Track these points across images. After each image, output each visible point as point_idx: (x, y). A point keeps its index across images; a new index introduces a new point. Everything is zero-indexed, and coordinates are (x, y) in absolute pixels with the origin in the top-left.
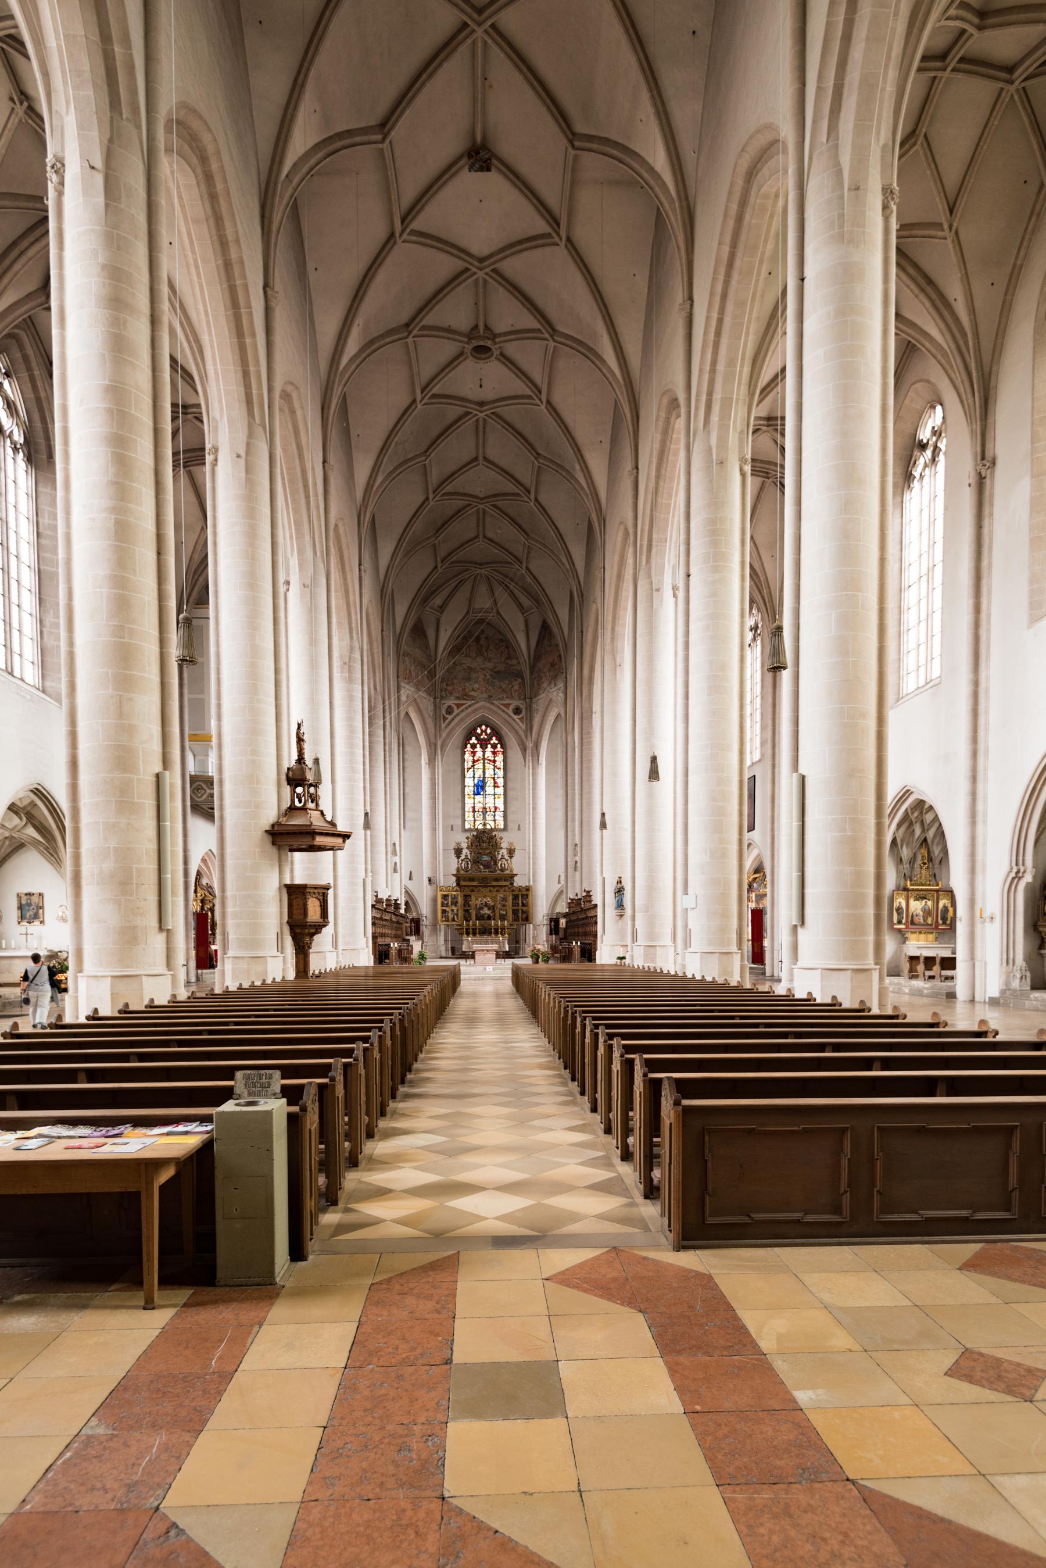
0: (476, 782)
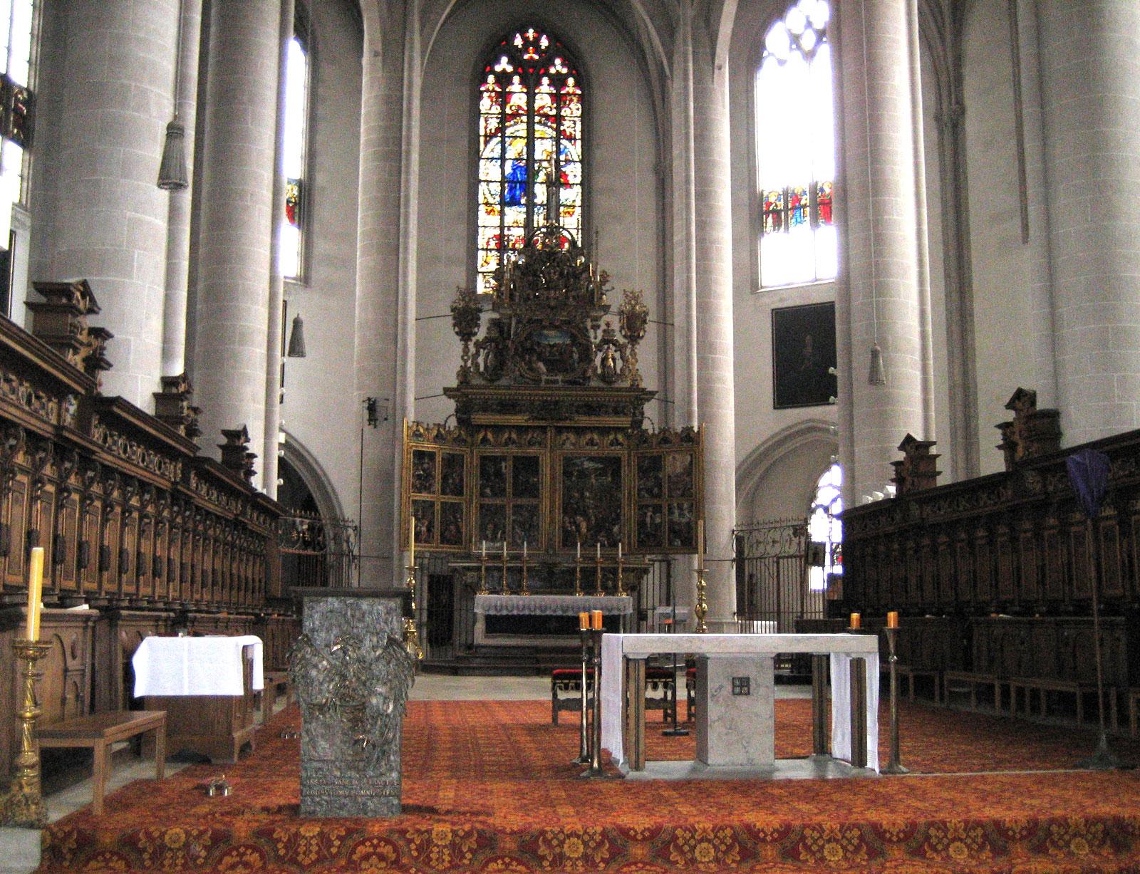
0: (508, 170)
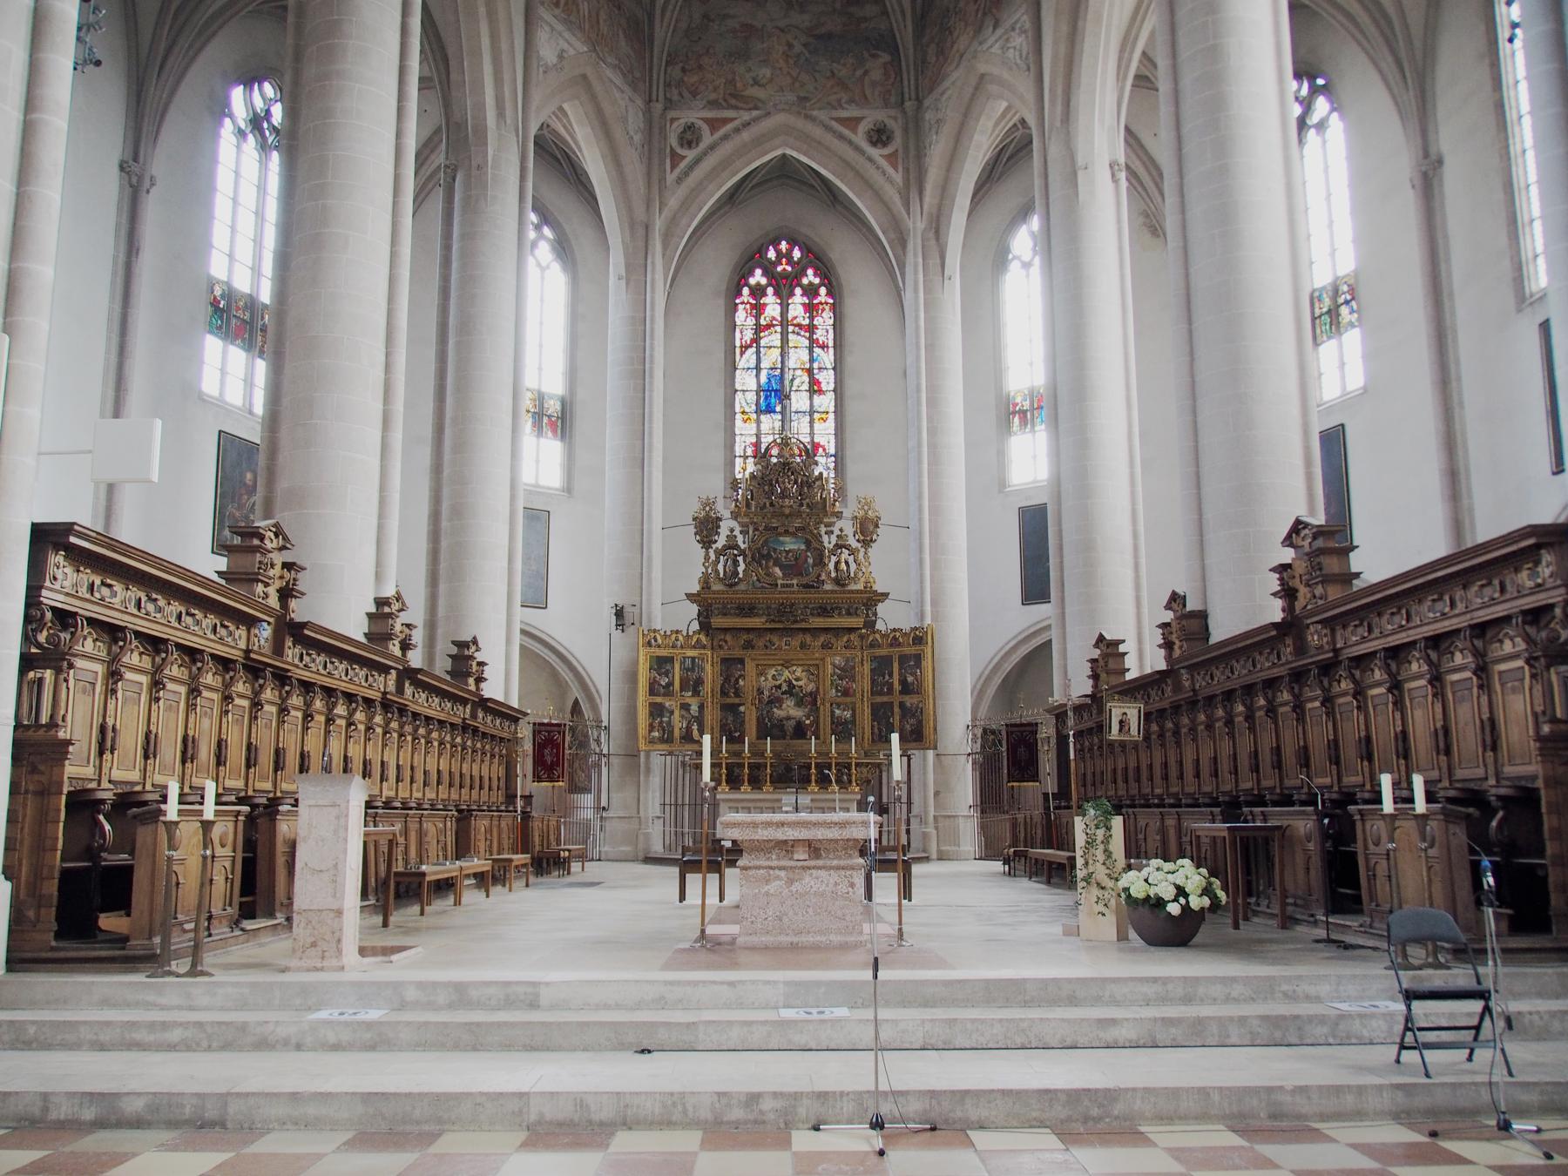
0: (763, 379)
